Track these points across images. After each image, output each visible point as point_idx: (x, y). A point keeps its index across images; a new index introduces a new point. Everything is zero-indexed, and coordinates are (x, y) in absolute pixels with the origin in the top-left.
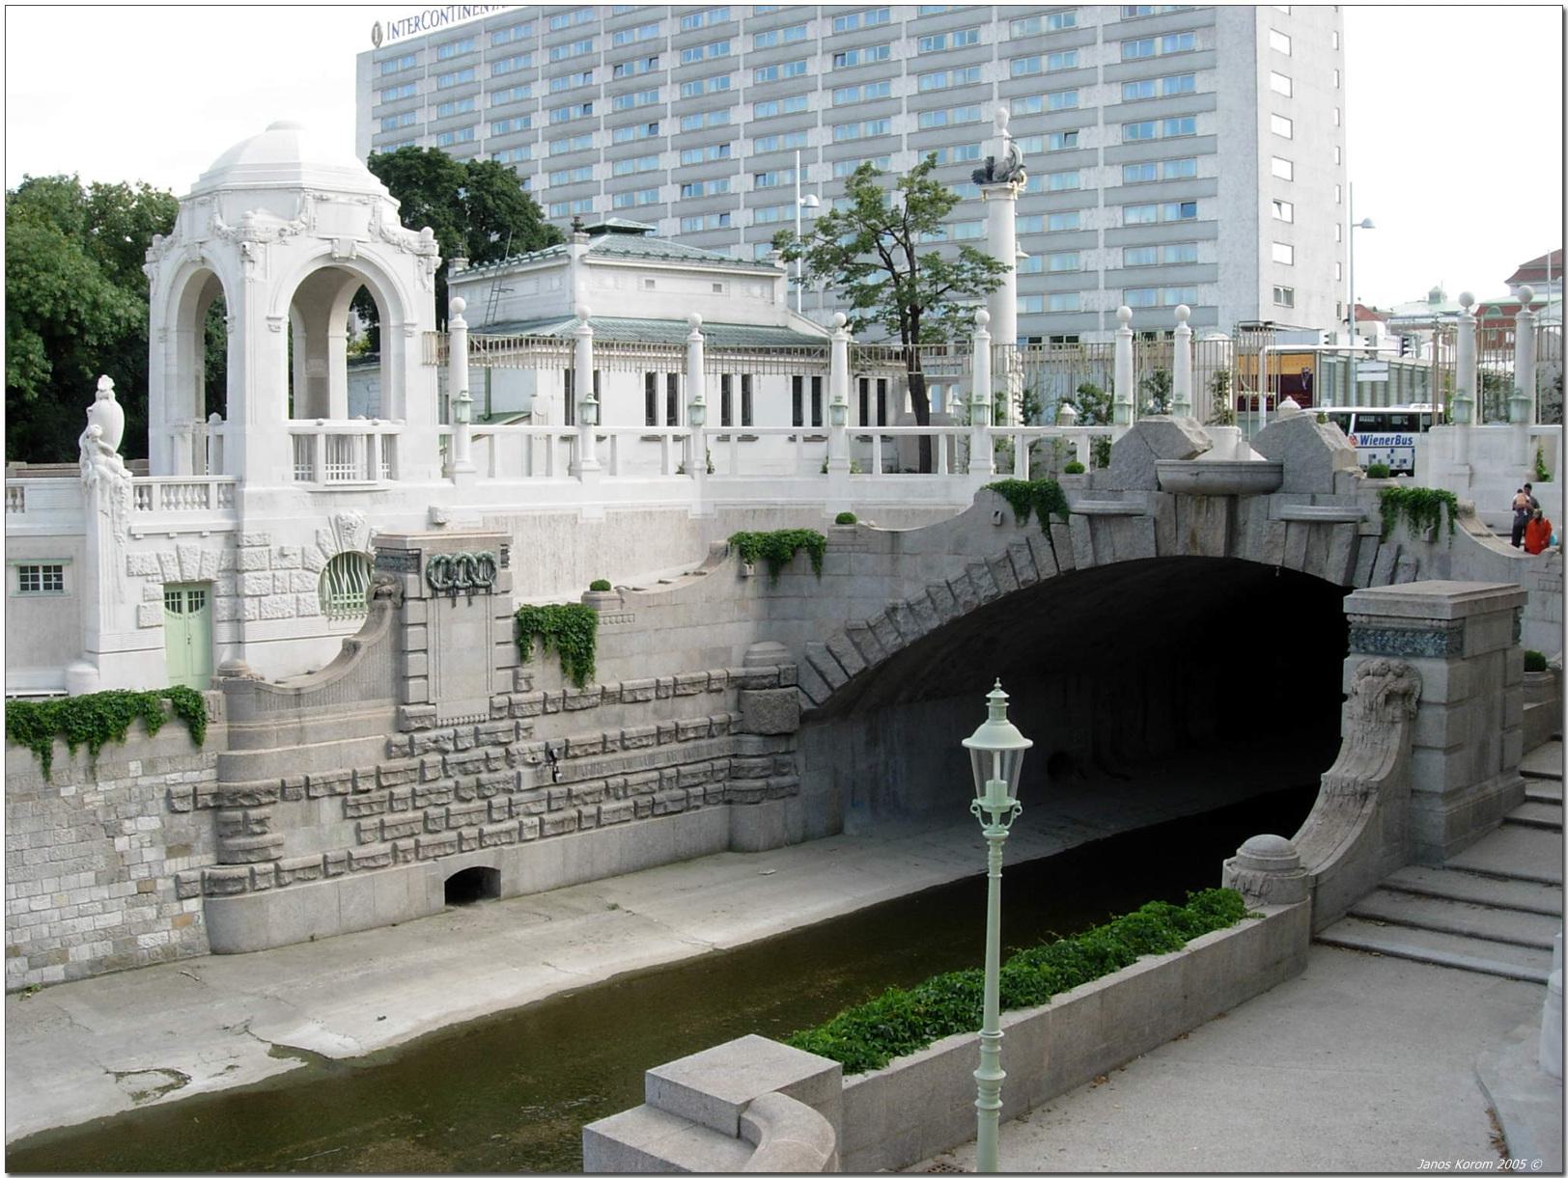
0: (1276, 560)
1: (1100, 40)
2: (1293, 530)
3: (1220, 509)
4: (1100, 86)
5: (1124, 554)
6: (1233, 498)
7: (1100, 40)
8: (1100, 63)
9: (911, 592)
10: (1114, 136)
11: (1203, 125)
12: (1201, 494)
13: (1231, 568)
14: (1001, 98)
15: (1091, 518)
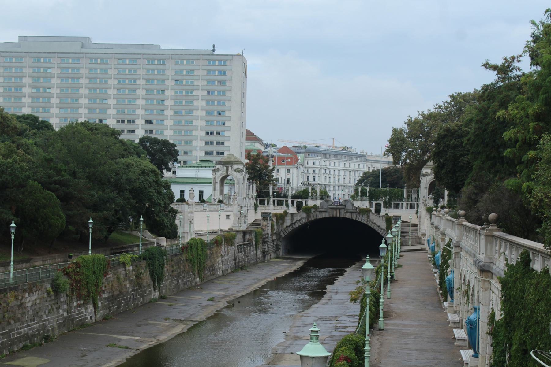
0: (346, 217)
1: (200, 99)
2: (349, 214)
3: (338, 211)
4: (200, 111)
5: (324, 217)
6: (340, 209)
7: (200, 99)
8: (200, 105)
9: (294, 221)
10: (203, 123)
11: (227, 124)
12: (336, 209)
13: (339, 218)
14: (171, 109)
15: (320, 212)
